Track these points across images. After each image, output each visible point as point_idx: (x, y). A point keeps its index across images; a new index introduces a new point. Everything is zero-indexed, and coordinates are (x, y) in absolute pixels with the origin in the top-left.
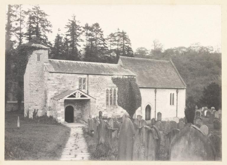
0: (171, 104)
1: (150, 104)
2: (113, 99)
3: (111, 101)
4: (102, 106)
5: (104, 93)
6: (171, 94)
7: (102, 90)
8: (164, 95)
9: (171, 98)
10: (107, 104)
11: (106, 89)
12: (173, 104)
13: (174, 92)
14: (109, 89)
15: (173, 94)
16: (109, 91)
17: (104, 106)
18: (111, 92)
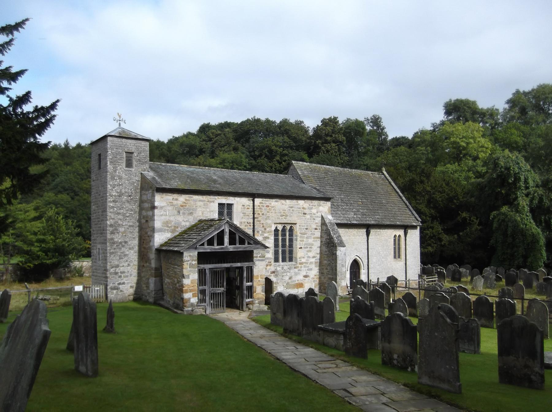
0: (395, 257)
1: (358, 258)
2: (287, 249)
3: (284, 252)
4: (267, 265)
6: (395, 236)
7: (265, 229)
9: (395, 244)
10: (276, 260)
11: (273, 228)
12: (399, 257)
13: (401, 232)
14: (280, 228)
15: (399, 236)
16: (280, 233)
17: (270, 265)
18: (284, 235)
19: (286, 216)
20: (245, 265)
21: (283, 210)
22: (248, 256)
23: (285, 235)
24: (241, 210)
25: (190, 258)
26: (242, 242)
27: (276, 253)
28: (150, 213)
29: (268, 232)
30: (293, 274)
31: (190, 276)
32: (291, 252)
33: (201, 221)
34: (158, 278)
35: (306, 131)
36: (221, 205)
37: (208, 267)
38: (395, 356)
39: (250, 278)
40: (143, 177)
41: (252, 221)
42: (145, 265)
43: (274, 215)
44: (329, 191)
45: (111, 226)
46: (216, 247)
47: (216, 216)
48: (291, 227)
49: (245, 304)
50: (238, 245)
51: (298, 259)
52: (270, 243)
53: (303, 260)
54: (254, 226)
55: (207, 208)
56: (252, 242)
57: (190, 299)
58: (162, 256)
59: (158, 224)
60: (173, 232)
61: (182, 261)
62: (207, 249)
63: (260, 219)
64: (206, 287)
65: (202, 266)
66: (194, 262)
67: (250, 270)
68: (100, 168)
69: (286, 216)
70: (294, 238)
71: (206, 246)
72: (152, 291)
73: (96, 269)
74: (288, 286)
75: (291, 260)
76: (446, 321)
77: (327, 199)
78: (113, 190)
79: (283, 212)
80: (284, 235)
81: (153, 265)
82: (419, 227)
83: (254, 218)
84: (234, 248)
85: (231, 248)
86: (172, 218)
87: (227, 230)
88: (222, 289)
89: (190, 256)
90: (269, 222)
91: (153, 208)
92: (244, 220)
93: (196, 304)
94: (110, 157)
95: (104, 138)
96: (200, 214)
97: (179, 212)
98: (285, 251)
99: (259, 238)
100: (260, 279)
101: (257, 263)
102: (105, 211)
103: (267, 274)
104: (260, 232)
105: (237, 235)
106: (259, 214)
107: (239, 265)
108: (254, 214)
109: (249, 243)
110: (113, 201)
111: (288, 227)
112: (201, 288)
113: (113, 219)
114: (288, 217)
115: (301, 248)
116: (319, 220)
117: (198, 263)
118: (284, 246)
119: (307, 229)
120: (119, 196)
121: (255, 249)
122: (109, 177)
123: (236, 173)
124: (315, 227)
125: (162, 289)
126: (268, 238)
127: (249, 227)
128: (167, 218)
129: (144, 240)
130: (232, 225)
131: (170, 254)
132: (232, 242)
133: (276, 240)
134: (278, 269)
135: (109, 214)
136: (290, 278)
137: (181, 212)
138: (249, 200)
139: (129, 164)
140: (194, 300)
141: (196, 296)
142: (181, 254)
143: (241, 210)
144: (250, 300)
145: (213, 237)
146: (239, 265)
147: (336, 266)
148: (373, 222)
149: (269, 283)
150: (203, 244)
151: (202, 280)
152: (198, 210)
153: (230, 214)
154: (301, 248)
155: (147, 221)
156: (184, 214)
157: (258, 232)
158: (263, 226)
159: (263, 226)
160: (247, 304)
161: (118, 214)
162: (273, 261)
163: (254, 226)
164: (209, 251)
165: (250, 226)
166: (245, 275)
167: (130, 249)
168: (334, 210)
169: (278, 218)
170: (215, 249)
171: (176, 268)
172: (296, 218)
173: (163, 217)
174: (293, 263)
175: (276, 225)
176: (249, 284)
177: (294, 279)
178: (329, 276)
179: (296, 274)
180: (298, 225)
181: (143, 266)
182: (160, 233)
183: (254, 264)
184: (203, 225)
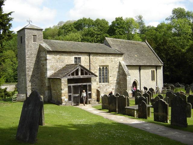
6: (152, 71)
7: (95, 68)
8: (146, 73)
9: (152, 74)
10: (100, 82)
12: (154, 80)
14: (101, 68)
20: (88, 84)
22: (89, 80)
23: (104, 71)
24: (84, 61)
25: (64, 81)
26: (86, 74)
27: (100, 79)
28: (44, 62)
32: (106, 78)
34: (49, 91)
35: (107, 23)
36: (76, 58)
37: (72, 85)
38: (160, 117)
40: (40, 46)
41: (89, 65)
42: (43, 85)
44: (123, 51)
45: (28, 68)
46: (75, 77)
47: (73, 63)
49: (88, 101)
51: (110, 82)
52: (97, 74)
53: (112, 82)
55: (70, 60)
59: (48, 67)
60: (55, 70)
61: (61, 83)
62: (71, 77)
63: (92, 64)
65: (69, 85)
67: (90, 86)
68: (21, 42)
71: (71, 76)
72: (47, 96)
73: (21, 87)
76: (182, 100)
77: (121, 54)
78: (28, 52)
81: (47, 85)
82: (162, 67)
84: (83, 77)
85: (82, 77)
86: (55, 64)
87: (80, 69)
88: (79, 94)
90: (97, 65)
91: (46, 60)
94: (26, 38)
95: (23, 29)
98: (104, 78)
102: (25, 61)
103: (97, 88)
105: (85, 71)
107: (85, 84)
108: (90, 61)
109: (89, 74)
110: (28, 57)
112: (69, 94)
113: (28, 65)
115: (111, 76)
116: (118, 64)
119: (113, 68)
120: (31, 55)
121: (92, 77)
122: (26, 46)
123: (94, 44)
124: (116, 67)
126: (96, 72)
128: (52, 64)
130: (81, 66)
131: (55, 80)
132: (82, 74)
133: (100, 73)
134: (101, 86)
135: (27, 63)
136: (106, 90)
137: (58, 61)
138: (88, 56)
139: (34, 41)
140: (67, 99)
141: (67, 98)
142: (60, 79)
143: (84, 61)
144: (90, 99)
146: (85, 84)
147: (127, 84)
148: (142, 64)
149: (98, 92)
151: (69, 91)
153: (80, 62)
154: (111, 76)
155: (43, 66)
156: (60, 62)
158: (94, 67)
159: (94, 67)
160: (89, 101)
161: (31, 63)
162: (98, 82)
164: (72, 78)
166: (88, 88)
167: (36, 78)
168: (124, 60)
170: (74, 77)
171: (58, 86)
173: (50, 64)
176: (90, 92)
178: (123, 89)
179: (109, 88)
181: (42, 85)
184: (68, 66)
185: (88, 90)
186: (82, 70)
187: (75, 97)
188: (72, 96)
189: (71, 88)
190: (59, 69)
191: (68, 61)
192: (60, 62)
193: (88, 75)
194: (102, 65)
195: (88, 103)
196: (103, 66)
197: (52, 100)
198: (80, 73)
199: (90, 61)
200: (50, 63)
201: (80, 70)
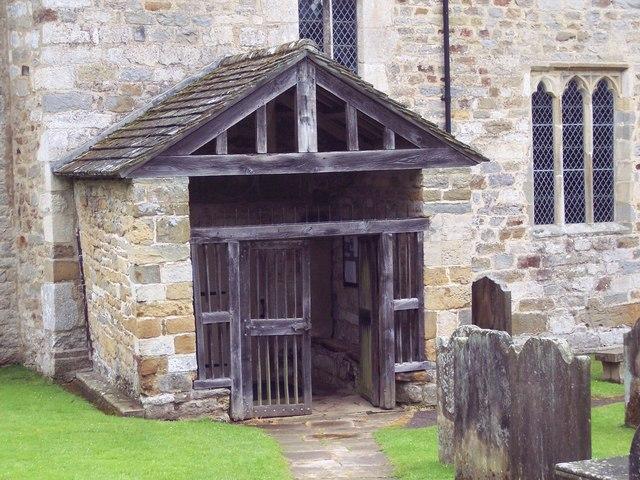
2: (588, 170)
3: (573, 184)
4: (504, 235)
5: (514, 120)
7: (495, 93)
10: (543, 214)
11: (528, 89)
14: (557, 86)
17: (518, 235)
18: (573, 114)
19: (583, 38)
20: (388, 227)
21: (568, 16)
22: (397, 192)
26: (371, 137)
29: (508, 104)
30: (613, 268)
31: (164, 272)
32: (605, 182)
33: (226, 64)
34: (68, 286)
39: (412, 280)
41: (436, 60)
43: (528, 33)
48: (603, 84)
50: (354, 151)
52: (514, 150)
54: (447, 79)
56: (413, 138)
57: (162, 362)
58: (78, 199)
60: (118, 109)
62: (227, 163)
64: (229, 315)
65: (212, 232)
66: (175, 219)
67: (411, 249)
69: (583, 38)
70: (618, 125)
71: (223, 153)
74: (593, 315)
75: (604, 212)
79: (566, 22)
80: (573, 114)
81: (49, 237)
83: (447, 49)
84: (339, 162)
85: (328, 162)
86: (114, 55)
87: (309, 92)
89: (158, 192)
90: (509, 62)
92: (403, 59)
93: (190, 378)
96: (228, 35)
97: (142, 31)
99: (466, 131)
100: (451, 284)
101: (436, 220)
104: (475, 105)
106: (467, 33)
107: (362, 227)
108: (446, 32)
111: (590, 87)
112: (209, 315)
114: (589, 45)
117: (195, 222)
118: (574, 157)
121: (426, 164)
125: (86, 327)
126: (507, 127)
127: (427, 84)
128: (97, 53)
129: (20, 141)
132: (329, 139)
133: (542, 137)
134: (552, 248)
137: (150, 30)
140: (183, 364)
141: (188, 350)
145: (250, 121)
146: (362, 227)
149: (488, 302)
150: (210, 148)
152: (219, 20)
155: (25, 69)
157: (465, 103)
158: (486, 82)
159: (486, 82)
162: (528, 217)
163: (447, 79)
165: (432, 79)
166: (389, 267)
169: (548, 48)
170: (260, 165)
172: (625, 48)
173: (81, 52)
174: (614, 226)
175: (538, 78)
177: (616, 288)
180: (630, 76)
182: (70, 114)
183: (425, 222)
185: (390, 286)
186: (329, 110)
187: (261, 347)
188: (235, 334)
189: (226, 263)
190: (160, 97)
191: (237, 30)
192: (162, 37)
193: (391, 150)
194: (568, 62)
195: (389, 396)
196: (574, 74)
197: (91, 363)
198: (307, 135)
199: (446, 32)
200: (74, 44)
201: (312, 105)
